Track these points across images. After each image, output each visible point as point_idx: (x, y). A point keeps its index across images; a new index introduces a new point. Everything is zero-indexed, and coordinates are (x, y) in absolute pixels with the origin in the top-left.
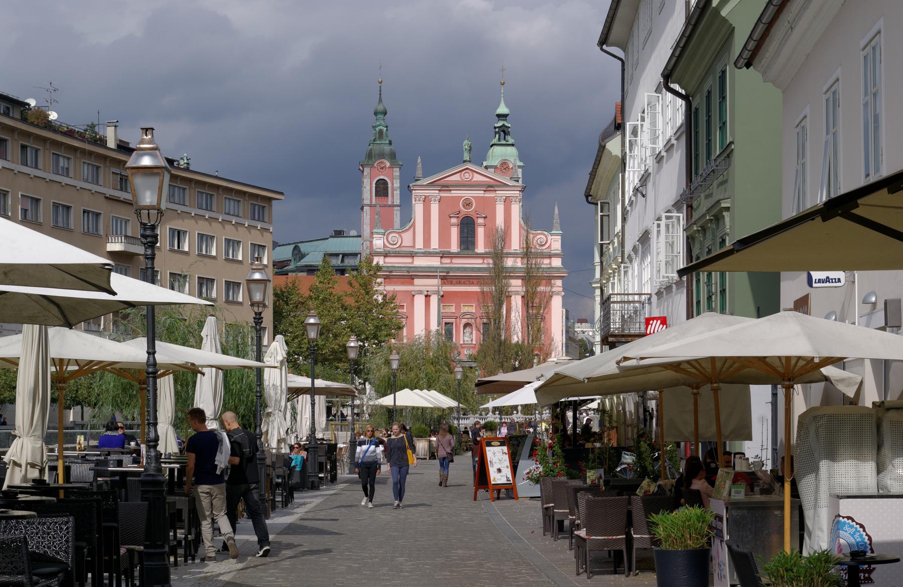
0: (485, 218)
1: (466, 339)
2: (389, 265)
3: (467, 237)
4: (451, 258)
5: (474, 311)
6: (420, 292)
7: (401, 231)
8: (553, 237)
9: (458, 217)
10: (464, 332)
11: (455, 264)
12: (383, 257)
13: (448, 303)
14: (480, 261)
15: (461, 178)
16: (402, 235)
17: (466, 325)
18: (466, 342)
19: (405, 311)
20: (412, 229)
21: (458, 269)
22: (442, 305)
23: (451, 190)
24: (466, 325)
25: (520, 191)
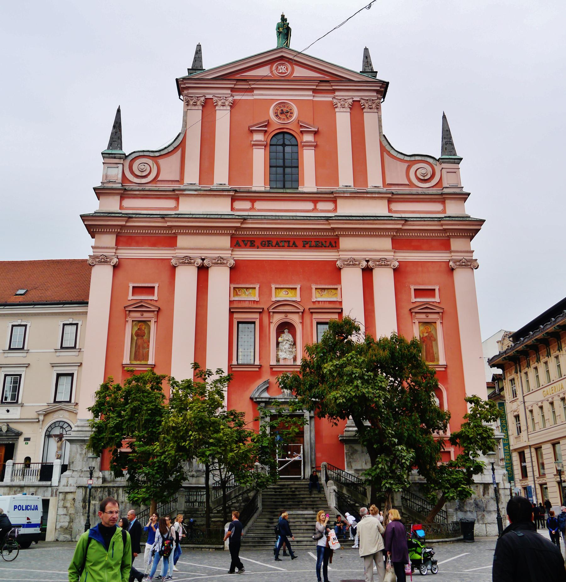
0: (316, 133)
1: (282, 355)
2: (131, 212)
3: (284, 167)
4: (253, 200)
5: (298, 299)
6: (187, 261)
7: (157, 154)
8: (444, 165)
9: (265, 132)
10: (278, 343)
11: (259, 210)
12: (118, 198)
13: (244, 282)
14: (309, 206)
15: (271, 72)
16: (161, 161)
18: (282, 362)
19: (155, 298)
20: (179, 152)
21: (265, 218)
22: (233, 286)
23: (251, 90)
25: (377, 92)
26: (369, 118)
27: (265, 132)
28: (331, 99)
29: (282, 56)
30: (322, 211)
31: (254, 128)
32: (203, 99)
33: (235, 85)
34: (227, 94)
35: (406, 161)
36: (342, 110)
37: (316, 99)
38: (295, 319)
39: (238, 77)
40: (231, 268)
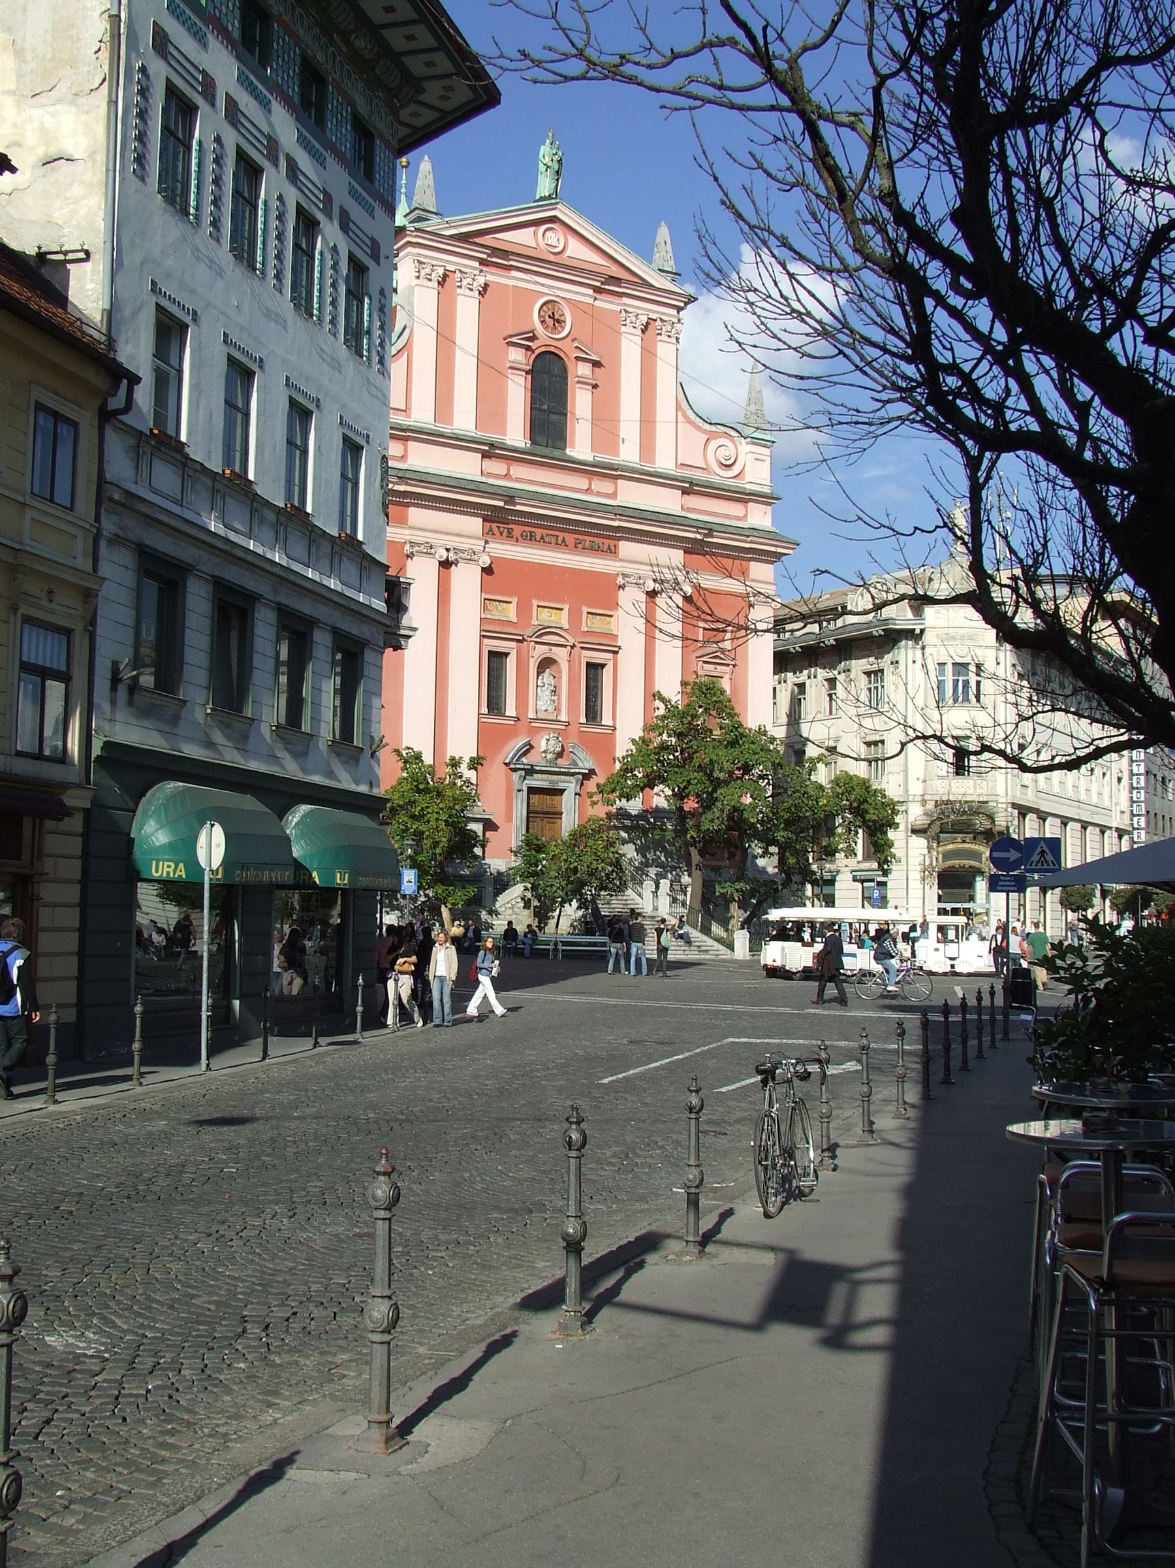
1: (542, 706)
9: (528, 348)
11: (518, 480)
14: (581, 482)
17: (546, 664)
24: (546, 664)
26: (665, 351)
27: (528, 348)
28: (618, 308)
29: (555, 216)
30: (599, 494)
31: (514, 340)
32: (441, 271)
33: (489, 255)
34: (475, 268)
35: (705, 432)
36: (632, 330)
37: (597, 303)
38: (561, 654)
39: (487, 240)
40: (483, 569)
